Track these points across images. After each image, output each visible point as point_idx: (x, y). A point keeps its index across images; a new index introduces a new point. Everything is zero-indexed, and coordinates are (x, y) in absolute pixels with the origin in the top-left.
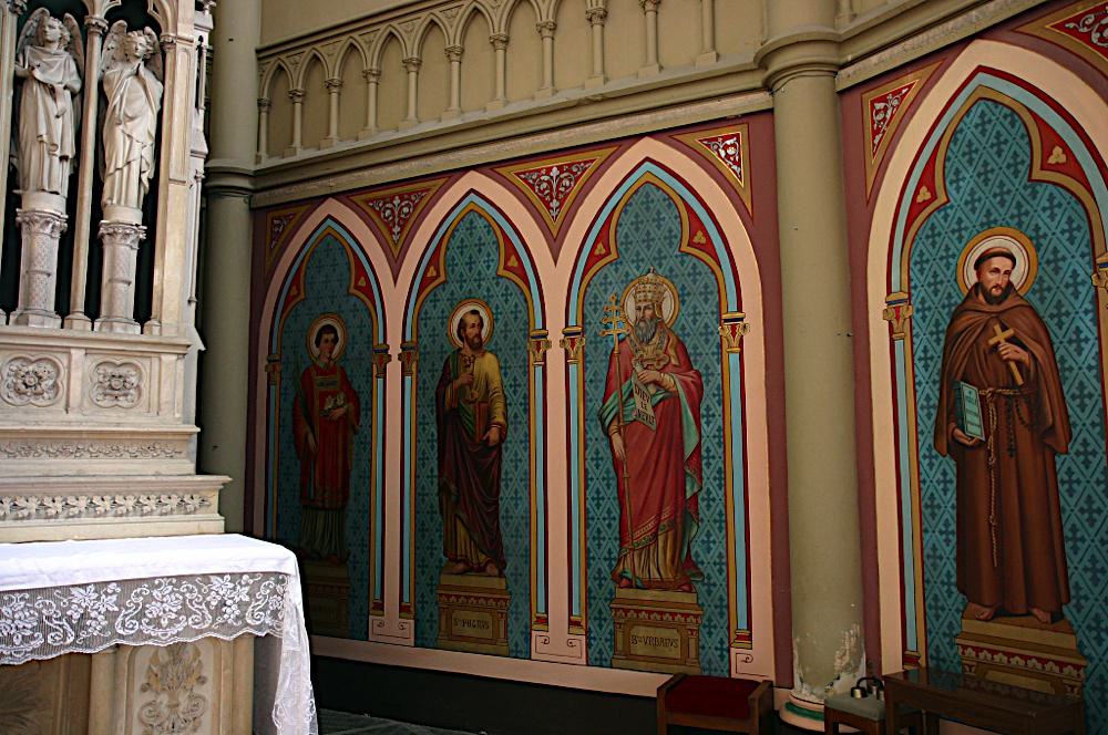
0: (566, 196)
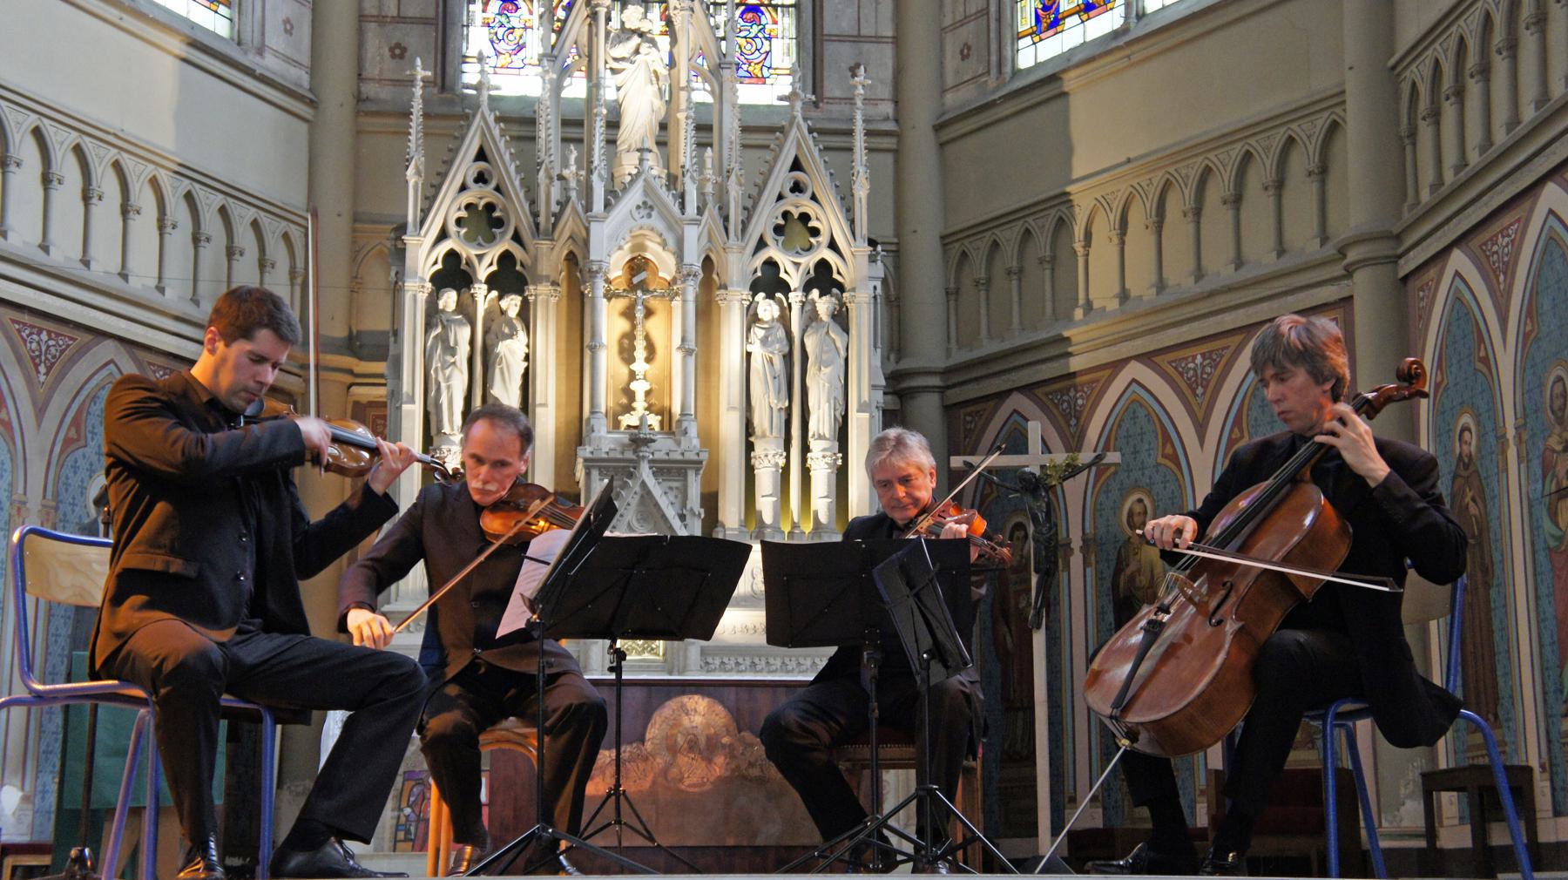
0: (1208, 382)
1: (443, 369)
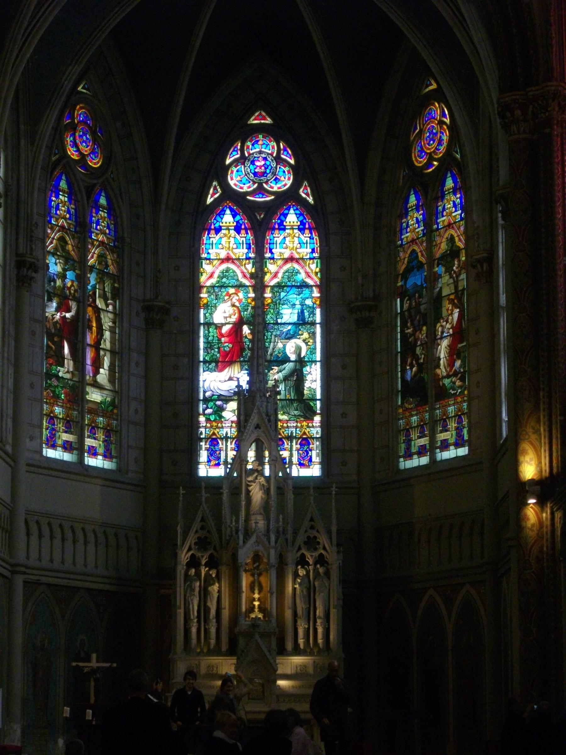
1: (191, 596)
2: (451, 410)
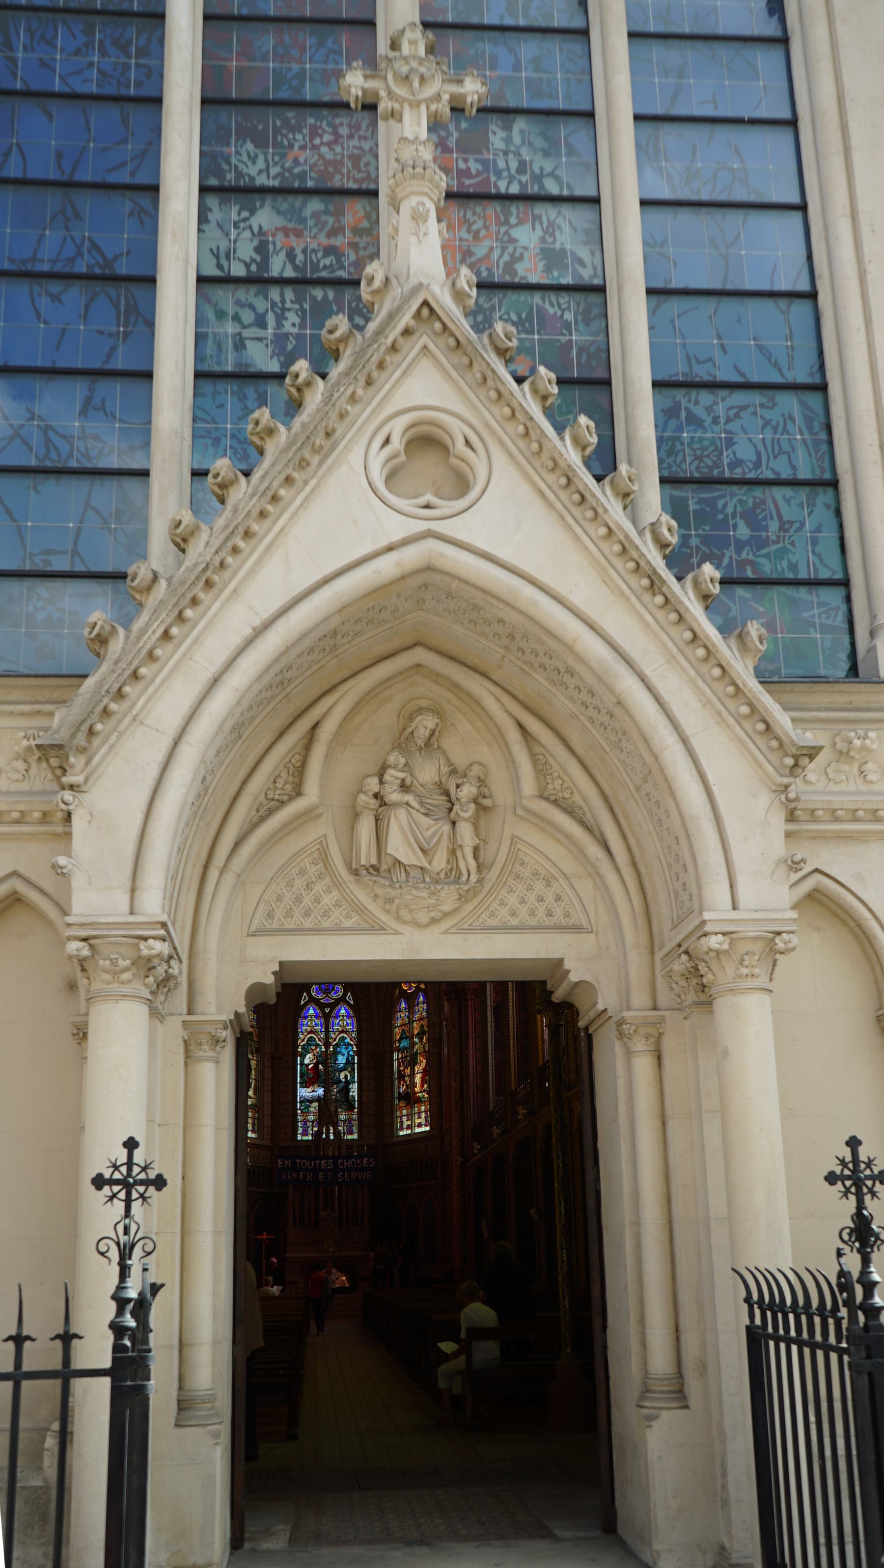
2: (423, 1108)
